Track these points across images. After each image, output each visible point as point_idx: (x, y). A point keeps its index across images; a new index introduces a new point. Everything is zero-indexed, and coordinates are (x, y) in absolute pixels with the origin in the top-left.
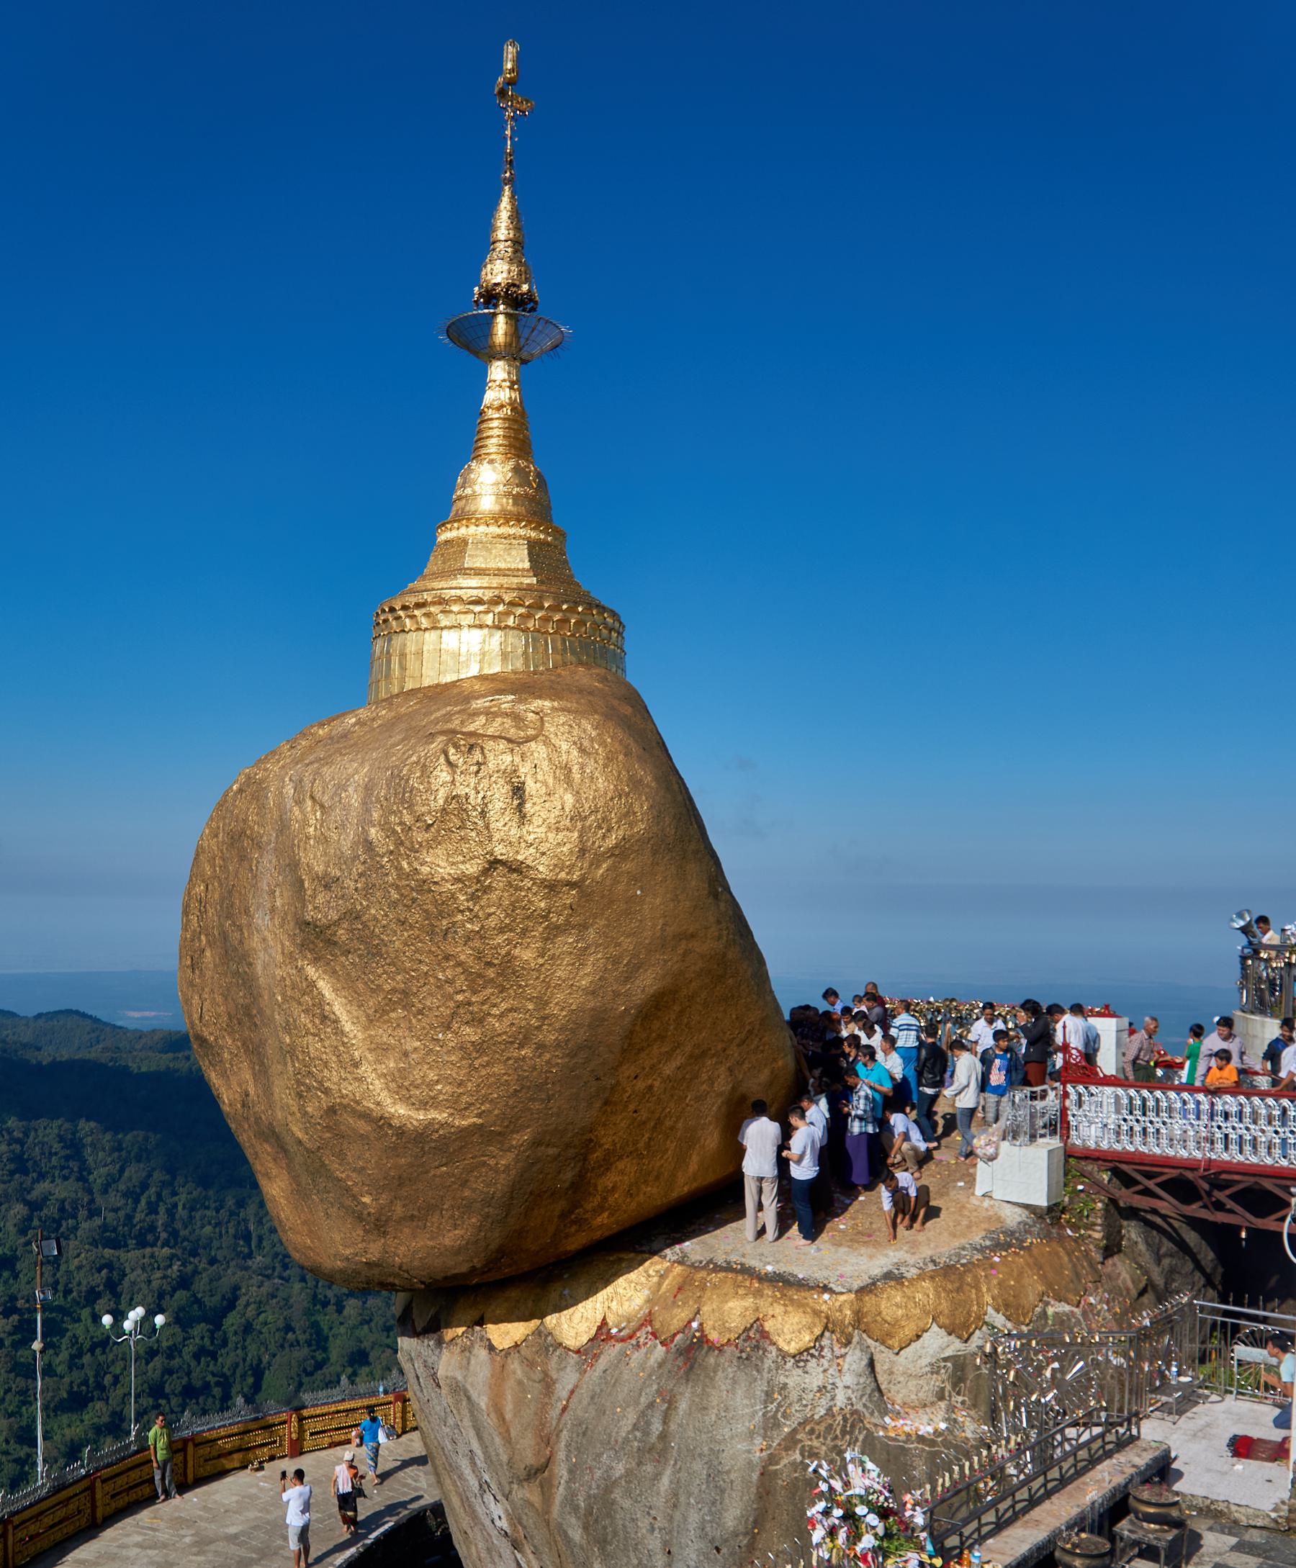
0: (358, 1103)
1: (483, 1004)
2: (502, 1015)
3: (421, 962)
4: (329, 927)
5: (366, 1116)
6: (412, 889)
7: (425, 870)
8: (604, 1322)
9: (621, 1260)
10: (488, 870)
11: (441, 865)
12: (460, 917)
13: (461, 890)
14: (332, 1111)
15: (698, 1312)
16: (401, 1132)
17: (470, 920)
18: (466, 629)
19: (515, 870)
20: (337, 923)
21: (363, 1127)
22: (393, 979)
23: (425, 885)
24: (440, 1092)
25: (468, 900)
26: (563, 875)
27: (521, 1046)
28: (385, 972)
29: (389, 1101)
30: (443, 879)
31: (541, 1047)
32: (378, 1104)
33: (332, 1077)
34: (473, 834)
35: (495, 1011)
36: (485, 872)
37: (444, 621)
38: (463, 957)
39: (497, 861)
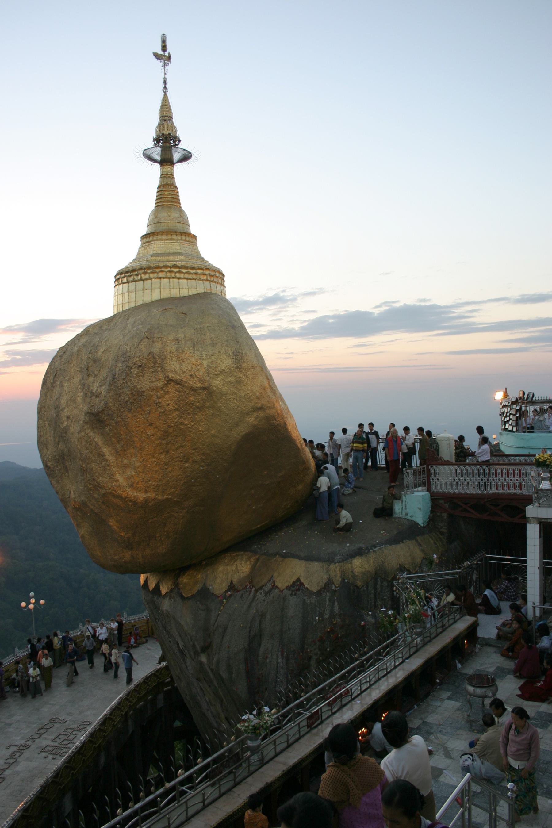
1: (168, 444)
2: (177, 449)
5: (119, 497)
8: (232, 582)
9: (237, 555)
10: (166, 384)
11: (144, 383)
14: (105, 495)
15: (272, 576)
16: (135, 503)
18: (153, 280)
19: (178, 384)
21: (118, 502)
24: (151, 485)
26: (199, 385)
27: (186, 462)
30: (147, 389)
31: (194, 462)
33: (103, 480)
36: (166, 385)
37: (144, 277)
38: (158, 424)
39: (171, 380)
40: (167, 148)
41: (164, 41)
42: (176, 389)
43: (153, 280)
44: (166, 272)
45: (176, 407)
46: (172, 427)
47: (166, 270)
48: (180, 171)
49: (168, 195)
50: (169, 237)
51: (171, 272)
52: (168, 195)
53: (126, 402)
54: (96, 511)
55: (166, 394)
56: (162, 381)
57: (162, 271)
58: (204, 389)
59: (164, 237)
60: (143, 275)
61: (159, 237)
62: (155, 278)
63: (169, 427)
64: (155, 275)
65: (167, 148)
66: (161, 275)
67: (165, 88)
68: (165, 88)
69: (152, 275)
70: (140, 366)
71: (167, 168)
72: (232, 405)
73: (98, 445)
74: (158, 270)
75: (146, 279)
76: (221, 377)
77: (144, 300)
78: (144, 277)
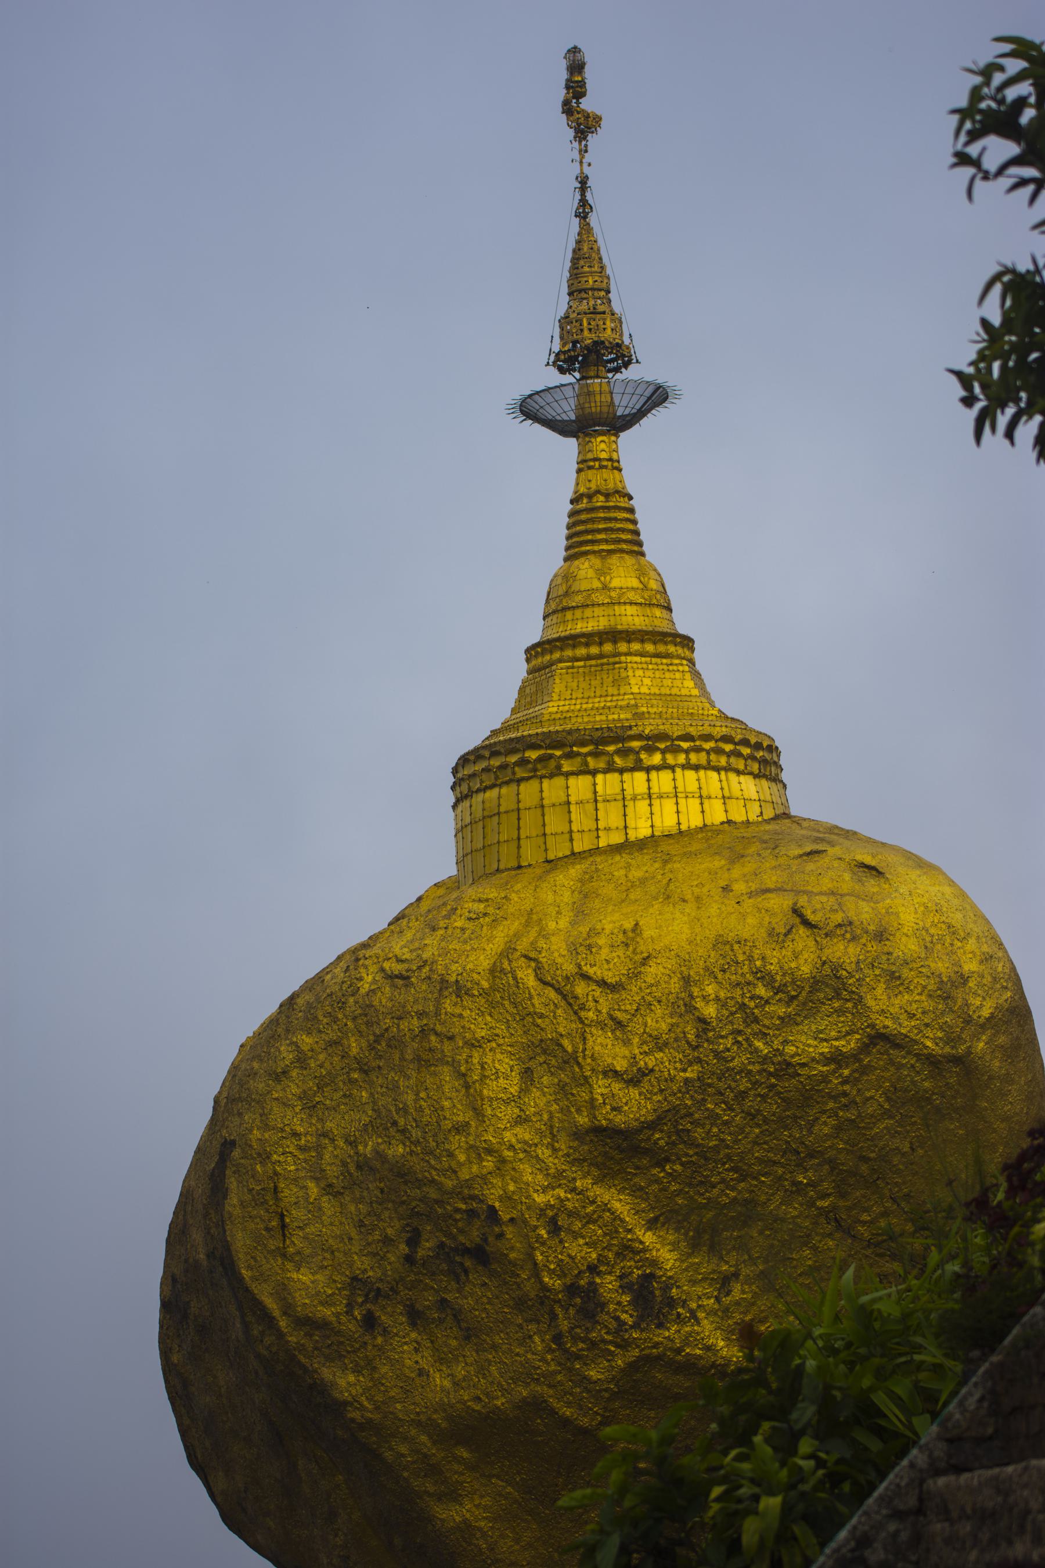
0: (679, 1351)
3: (775, 1163)
4: (639, 1131)
5: (689, 1367)
6: (770, 1074)
7: (790, 1049)
10: (867, 1046)
12: (831, 1105)
13: (834, 1071)
17: (845, 1107)
18: (678, 770)
20: (651, 1126)
22: (733, 1189)
23: (786, 1068)
25: (843, 1083)
28: (723, 1181)
29: (721, 1343)
30: (813, 1059)
32: (708, 1348)
34: (849, 1005)
35: (865, 1217)
36: (865, 1048)
40: (593, 382)
41: (576, 66)
42: (891, 1059)
43: (678, 770)
44: (708, 752)
45: (887, 1106)
46: (869, 1159)
47: (707, 746)
48: (641, 457)
49: (601, 523)
50: (661, 648)
51: (719, 751)
52: (601, 523)
53: (742, 1095)
54: (584, 1422)
55: (863, 1073)
56: (858, 1036)
57: (698, 750)
58: (957, 1060)
59: (650, 648)
60: (643, 756)
61: (636, 646)
62: (684, 767)
63: (865, 1159)
64: (682, 758)
65: (593, 382)
66: (694, 758)
67: (584, 202)
68: (584, 202)
69: (670, 759)
70: (793, 998)
71: (600, 445)
72: (1006, 1109)
73: (622, 1221)
74: (685, 745)
75: (658, 768)
76: (989, 1032)
77: (657, 823)
78: (670, 759)
